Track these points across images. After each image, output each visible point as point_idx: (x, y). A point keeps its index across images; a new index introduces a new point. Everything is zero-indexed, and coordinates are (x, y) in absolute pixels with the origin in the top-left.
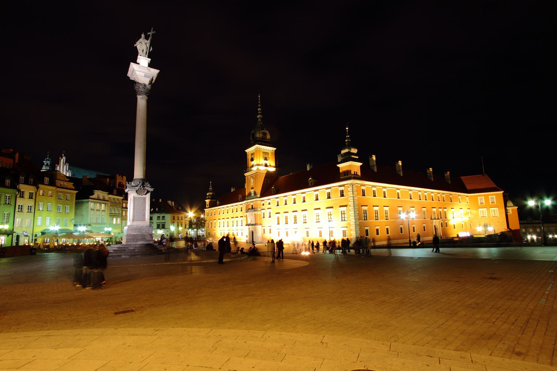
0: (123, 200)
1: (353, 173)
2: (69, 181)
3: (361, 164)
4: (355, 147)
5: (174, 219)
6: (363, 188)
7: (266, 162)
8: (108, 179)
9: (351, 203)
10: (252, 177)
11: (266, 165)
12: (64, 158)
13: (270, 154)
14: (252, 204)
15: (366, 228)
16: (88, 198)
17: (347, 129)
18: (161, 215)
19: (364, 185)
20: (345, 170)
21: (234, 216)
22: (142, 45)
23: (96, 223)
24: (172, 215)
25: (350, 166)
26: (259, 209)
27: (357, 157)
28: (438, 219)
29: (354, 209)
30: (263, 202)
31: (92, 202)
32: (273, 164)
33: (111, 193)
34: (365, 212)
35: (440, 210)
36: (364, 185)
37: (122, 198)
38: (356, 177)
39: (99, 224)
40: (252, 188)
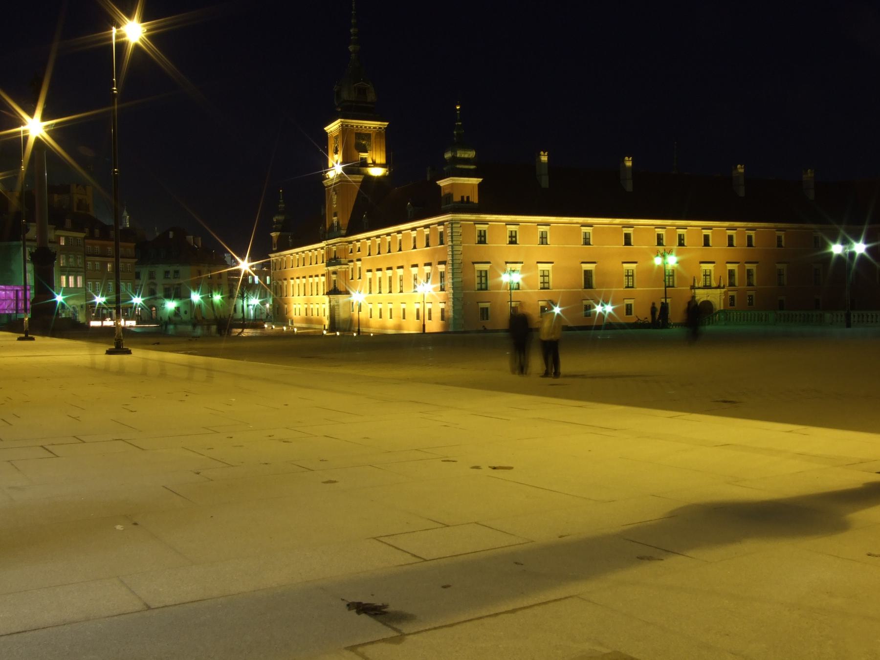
0: (85, 238)
1: (457, 198)
3: (480, 180)
4: (466, 147)
6: (480, 227)
9: (449, 258)
10: (334, 190)
13: (373, 138)
14: (334, 248)
15: (482, 305)
18: (171, 269)
19: (485, 223)
20: (447, 191)
21: (314, 274)
25: (452, 185)
26: (343, 260)
27: (472, 167)
28: (719, 287)
29: (453, 269)
30: (351, 246)
32: (381, 158)
34: (483, 275)
35: (730, 267)
36: (485, 223)
37: (82, 235)
38: (465, 207)
40: (335, 215)
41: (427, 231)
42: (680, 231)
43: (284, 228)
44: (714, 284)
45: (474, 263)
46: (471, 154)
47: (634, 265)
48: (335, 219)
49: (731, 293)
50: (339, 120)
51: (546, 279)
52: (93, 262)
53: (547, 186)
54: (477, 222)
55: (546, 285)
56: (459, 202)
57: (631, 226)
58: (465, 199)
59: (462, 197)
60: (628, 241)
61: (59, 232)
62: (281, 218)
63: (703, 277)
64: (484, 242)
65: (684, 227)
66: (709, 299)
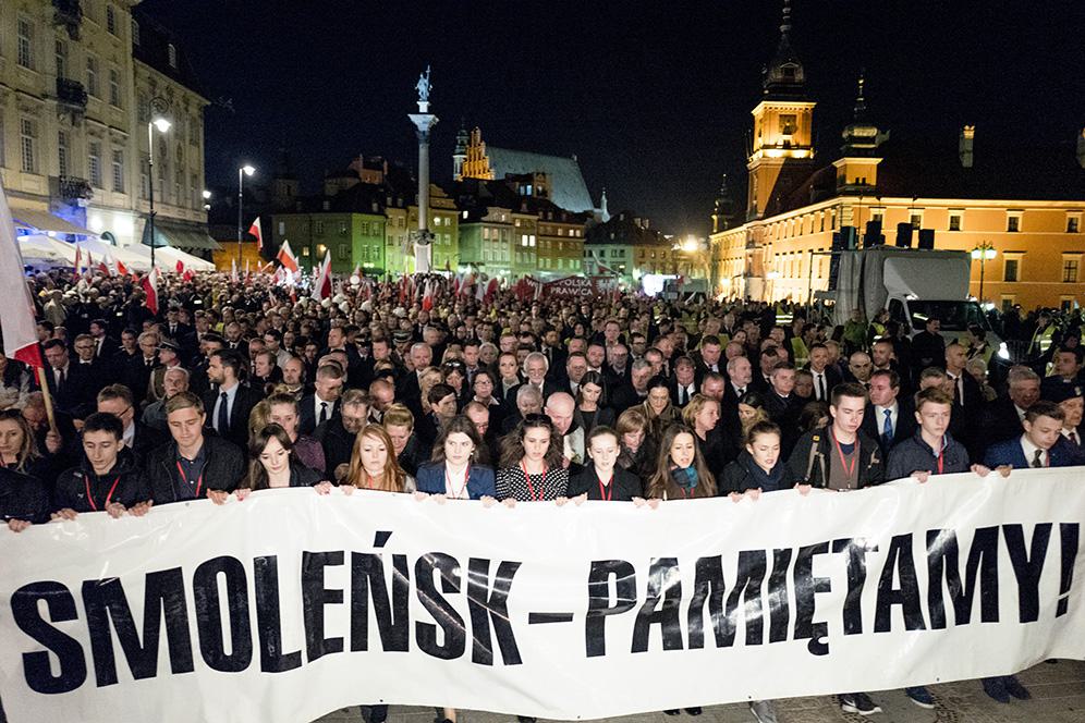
0: (539, 220)
2: (447, 198)
3: (880, 160)
5: (643, 256)
7: (787, 137)
8: (518, 184)
11: (787, 146)
12: (478, 131)
16: (479, 221)
17: (861, 82)
22: (423, 86)
23: (494, 262)
24: (639, 248)
31: (485, 227)
33: (516, 209)
37: (536, 218)
38: (861, 189)
39: (497, 263)
41: (822, 215)
42: (1070, 215)
43: (723, 211)
46: (873, 132)
47: (1080, 256)
48: (755, 202)
50: (763, 102)
52: (545, 241)
54: (872, 206)
58: (860, 182)
59: (857, 179)
61: (515, 215)
62: (723, 201)
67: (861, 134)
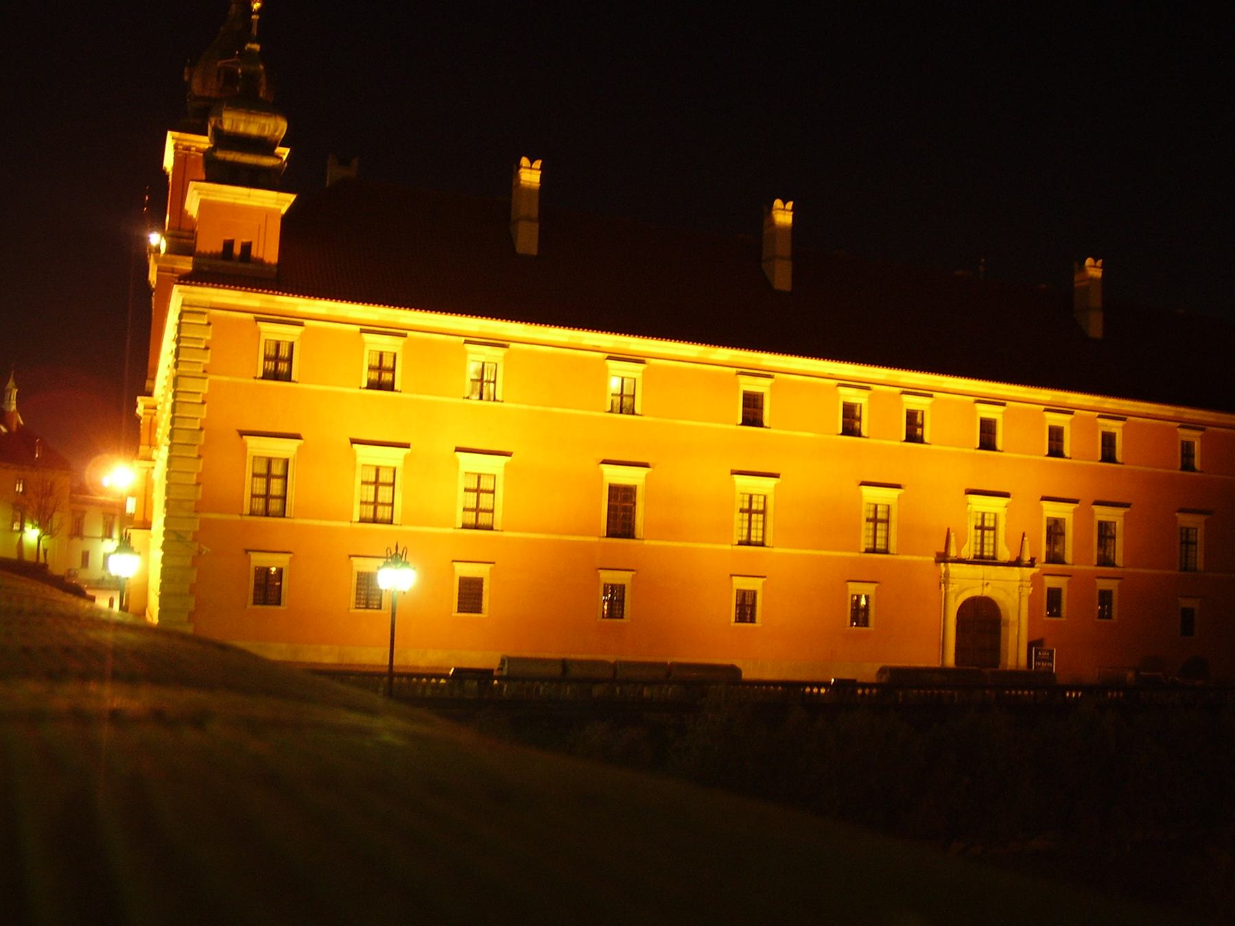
1: (210, 244)
3: (291, 198)
15: (259, 560)
17: (256, 6)
28: (1017, 563)
34: (270, 471)
35: (1052, 510)
44: (1005, 554)
45: (242, 433)
49: (1050, 582)
51: (385, 494)
53: (534, 251)
55: (484, 519)
56: (213, 256)
57: (765, 374)
58: (237, 250)
59: (229, 245)
60: (752, 411)
63: (972, 535)
64: (287, 377)
65: (926, 393)
66: (987, 592)
67: (241, 129)
